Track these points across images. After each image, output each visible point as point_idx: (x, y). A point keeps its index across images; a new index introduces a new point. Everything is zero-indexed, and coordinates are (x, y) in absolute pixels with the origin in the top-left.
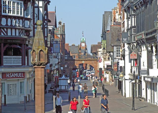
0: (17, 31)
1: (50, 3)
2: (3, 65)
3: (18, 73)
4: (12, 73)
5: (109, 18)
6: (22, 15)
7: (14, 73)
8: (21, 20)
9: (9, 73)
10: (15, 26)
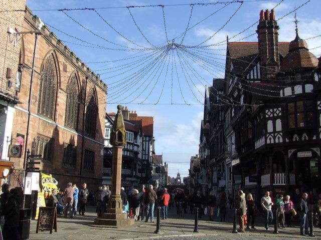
0: (128, 153)
8: (131, 146)
10: (127, 148)
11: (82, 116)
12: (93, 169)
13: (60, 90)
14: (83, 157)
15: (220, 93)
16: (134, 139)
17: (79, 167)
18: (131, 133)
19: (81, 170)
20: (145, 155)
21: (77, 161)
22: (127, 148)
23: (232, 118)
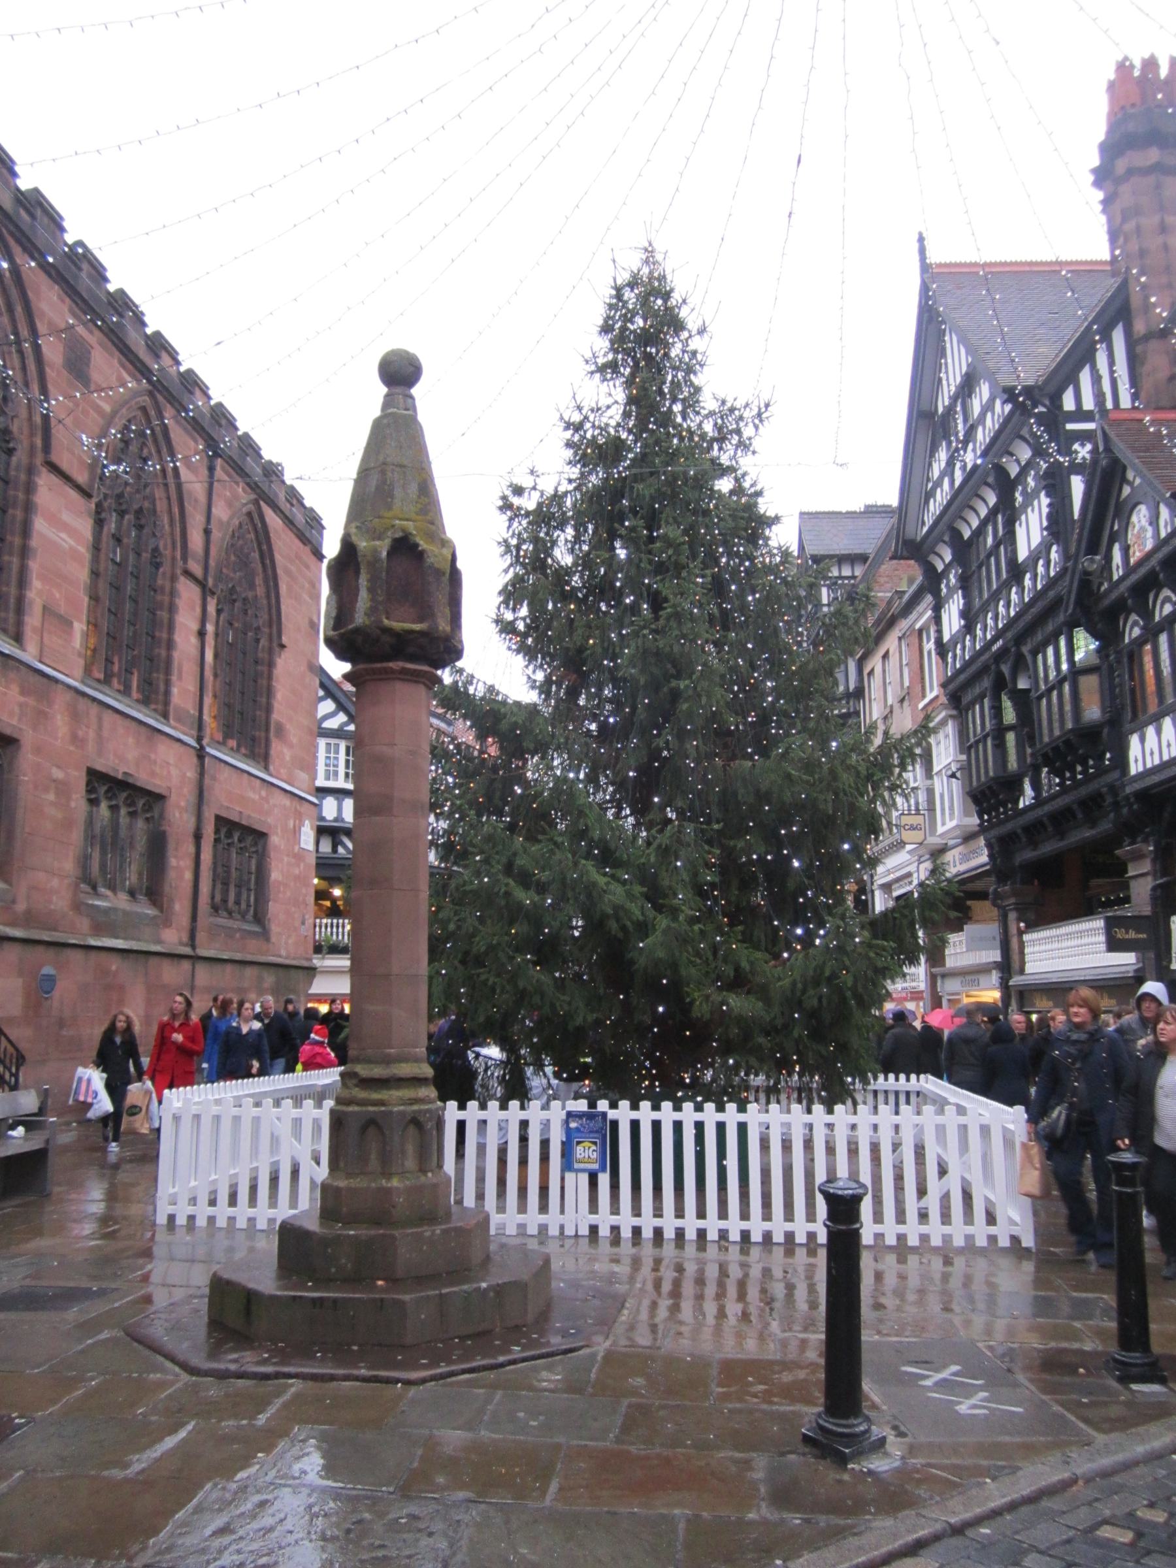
11: (194, 640)
12: (260, 918)
13: (45, 482)
17: (180, 908)
19: (194, 918)
21: (171, 875)
23: (942, 649)
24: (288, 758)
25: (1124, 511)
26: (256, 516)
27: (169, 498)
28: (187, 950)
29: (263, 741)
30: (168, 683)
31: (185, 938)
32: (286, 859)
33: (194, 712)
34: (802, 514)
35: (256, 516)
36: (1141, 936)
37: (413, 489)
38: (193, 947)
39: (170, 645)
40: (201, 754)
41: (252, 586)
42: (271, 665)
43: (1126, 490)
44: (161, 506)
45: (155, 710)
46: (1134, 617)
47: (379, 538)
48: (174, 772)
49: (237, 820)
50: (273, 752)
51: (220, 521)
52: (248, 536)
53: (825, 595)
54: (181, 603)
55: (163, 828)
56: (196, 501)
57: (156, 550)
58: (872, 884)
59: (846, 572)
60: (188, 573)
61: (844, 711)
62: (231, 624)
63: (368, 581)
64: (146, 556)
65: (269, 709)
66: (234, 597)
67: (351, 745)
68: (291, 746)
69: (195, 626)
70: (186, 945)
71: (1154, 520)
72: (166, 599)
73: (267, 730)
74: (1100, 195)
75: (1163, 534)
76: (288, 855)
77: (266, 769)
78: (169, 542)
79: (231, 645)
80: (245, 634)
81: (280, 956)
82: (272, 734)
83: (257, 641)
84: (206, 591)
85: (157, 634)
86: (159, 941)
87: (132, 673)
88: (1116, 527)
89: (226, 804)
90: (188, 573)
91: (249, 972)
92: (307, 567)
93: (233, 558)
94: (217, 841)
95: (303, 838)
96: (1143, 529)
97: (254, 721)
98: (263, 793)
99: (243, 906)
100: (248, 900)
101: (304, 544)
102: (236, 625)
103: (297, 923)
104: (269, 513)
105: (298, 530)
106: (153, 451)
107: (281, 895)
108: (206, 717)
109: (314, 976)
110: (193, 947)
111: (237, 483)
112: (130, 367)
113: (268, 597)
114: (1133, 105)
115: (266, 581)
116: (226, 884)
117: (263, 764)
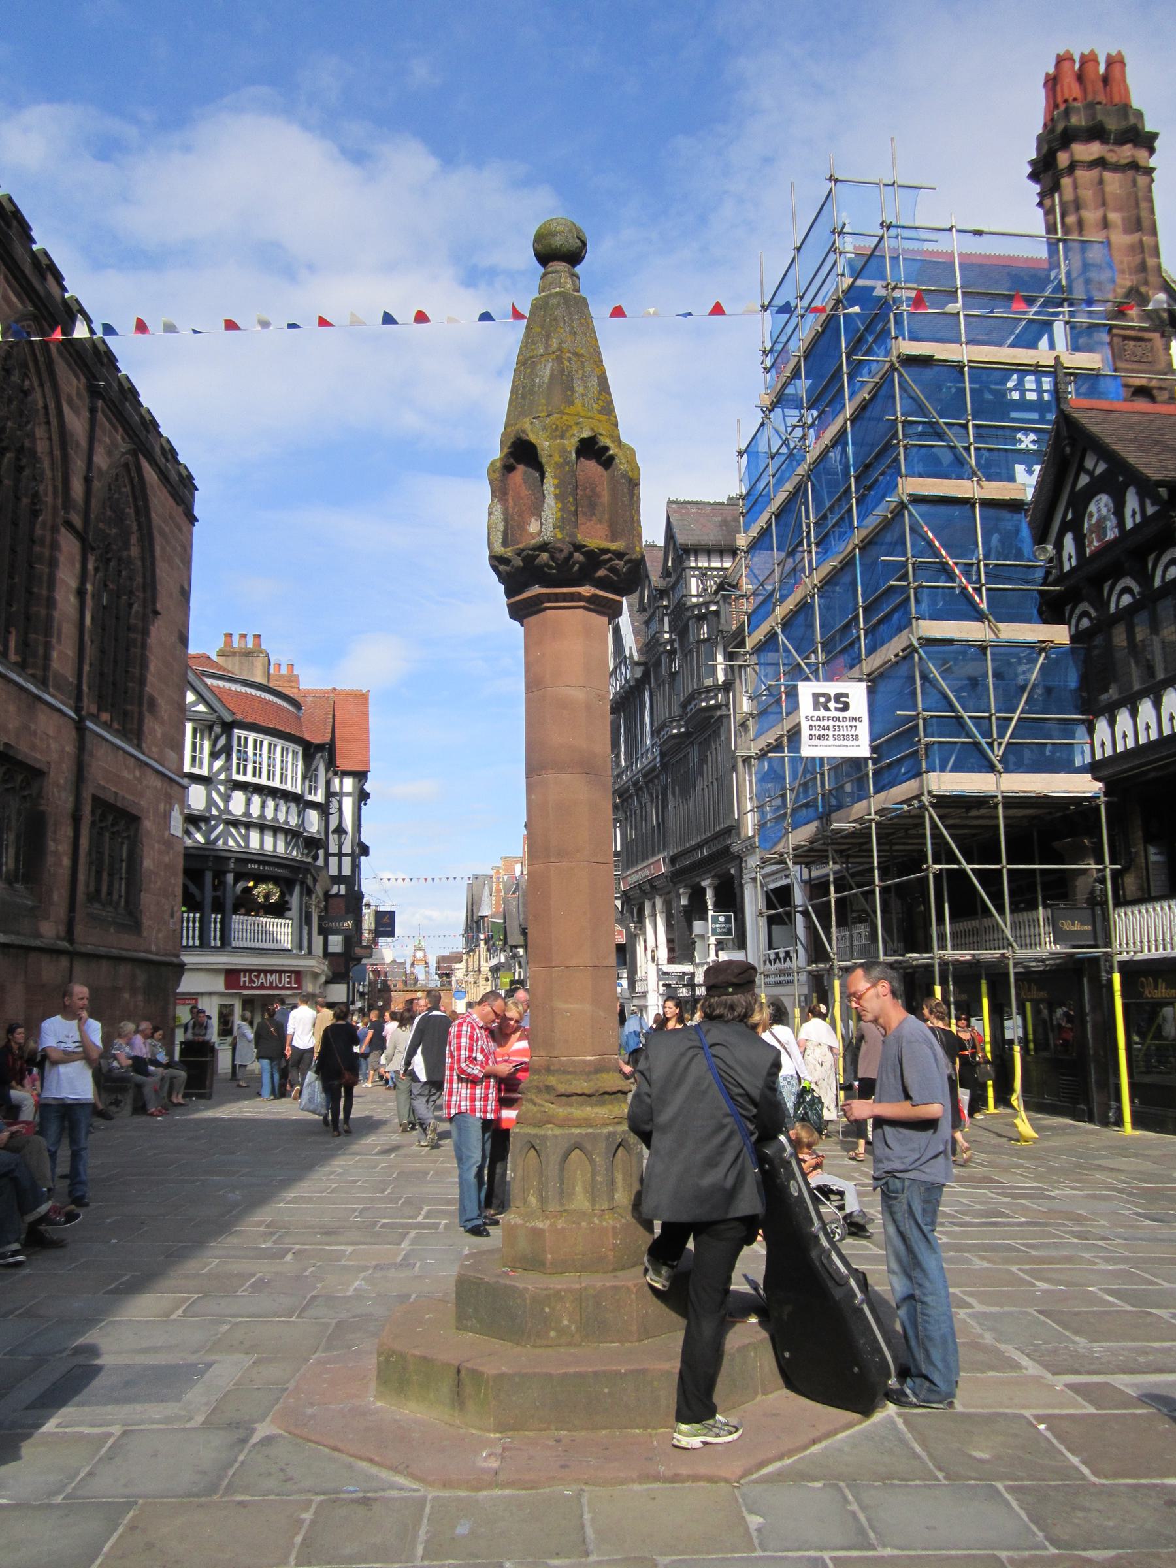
1: (368, 801)
2: (230, 944)
3: (281, 972)
4: (260, 971)
5: (487, 888)
6: (298, 791)
7: (266, 972)
9: (251, 971)
10: (275, 819)
11: (73, 599)
14: (84, 842)
15: (703, 563)
16: (304, 777)
17: (59, 896)
18: (292, 746)
19: (72, 908)
20: (340, 855)
21: (50, 860)
22: (275, 819)
24: (159, 735)
25: (1081, 502)
26: (132, 468)
27: (50, 439)
28: (65, 945)
29: (136, 715)
30: (48, 646)
31: (62, 930)
32: (157, 846)
33: (72, 679)
34: (670, 502)
35: (132, 468)
36: (1086, 928)
37: (593, 382)
38: (71, 941)
39: (51, 603)
40: (80, 728)
41: (126, 545)
42: (145, 633)
43: (1084, 480)
44: (41, 447)
45: (33, 676)
46: (1084, 606)
47: (562, 437)
48: (54, 746)
49: (112, 801)
50: (145, 729)
51: (99, 469)
52: (124, 490)
53: (694, 586)
54: (62, 558)
55: (42, 808)
56: (78, 445)
57: (36, 495)
58: (742, 878)
59: (716, 564)
60: (69, 525)
61: (712, 702)
62: (106, 585)
63: (556, 487)
64: (25, 501)
65: (142, 682)
66: (109, 556)
67: (199, 727)
68: (162, 723)
69: (73, 584)
70: (63, 940)
71: (1119, 512)
72: (47, 552)
73: (140, 704)
74: (1037, 188)
75: (1129, 524)
76: (159, 842)
77: (139, 747)
78: (50, 488)
79: (104, 607)
80: (118, 597)
81: (150, 952)
82: (145, 708)
83: (130, 605)
84: (86, 548)
85: (35, 590)
86: (38, 935)
87: (10, 633)
88: (1070, 516)
89: (102, 783)
90: (69, 525)
91: (124, 969)
92: (180, 530)
93: (109, 513)
94: (93, 823)
95: (172, 823)
96: (1102, 520)
97: (126, 693)
98: (137, 773)
99: (115, 897)
100: (120, 891)
101: (178, 504)
102: (111, 586)
103: (166, 916)
104: (145, 465)
105: (172, 486)
106: (36, 384)
107: (152, 885)
108: (85, 688)
109: (182, 974)
110: (71, 941)
111: (117, 431)
112: (16, 285)
113: (143, 559)
114: (1075, 99)
115: (141, 540)
116: (99, 873)
117: (135, 742)
